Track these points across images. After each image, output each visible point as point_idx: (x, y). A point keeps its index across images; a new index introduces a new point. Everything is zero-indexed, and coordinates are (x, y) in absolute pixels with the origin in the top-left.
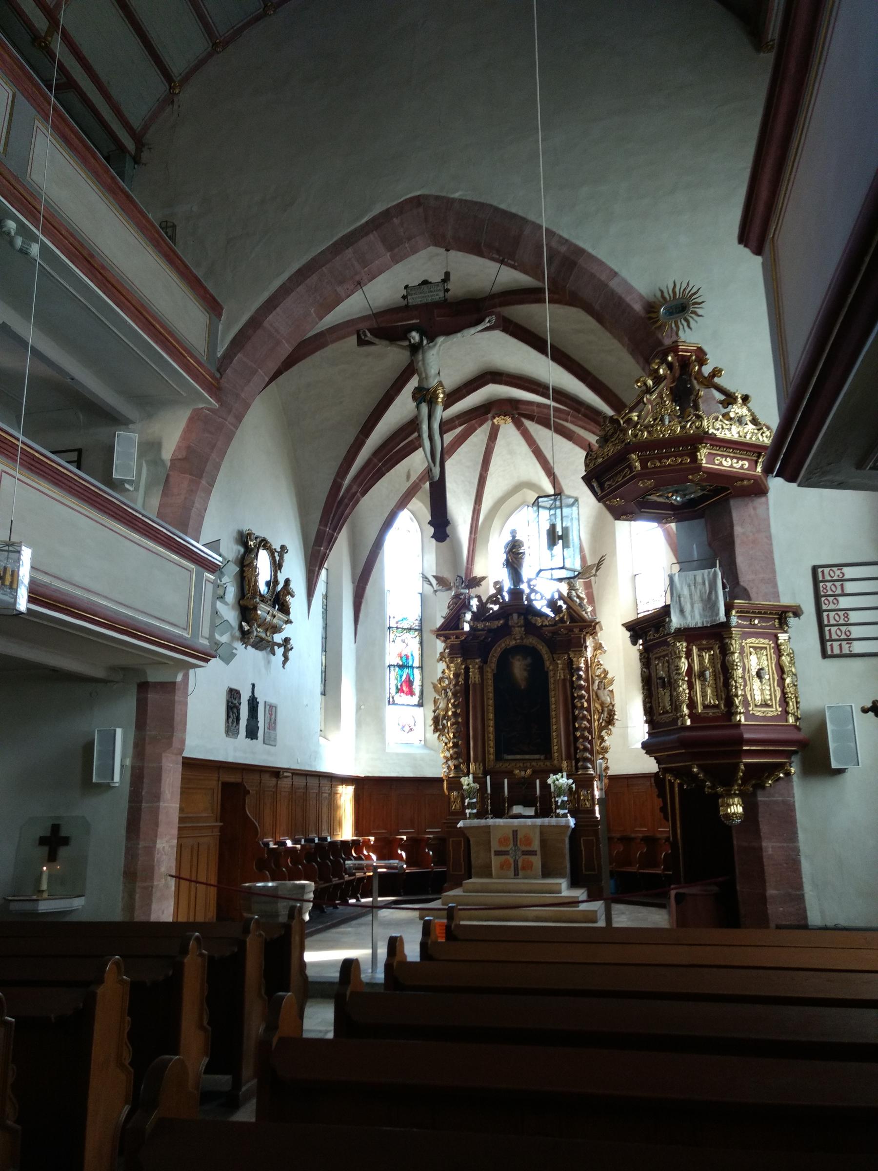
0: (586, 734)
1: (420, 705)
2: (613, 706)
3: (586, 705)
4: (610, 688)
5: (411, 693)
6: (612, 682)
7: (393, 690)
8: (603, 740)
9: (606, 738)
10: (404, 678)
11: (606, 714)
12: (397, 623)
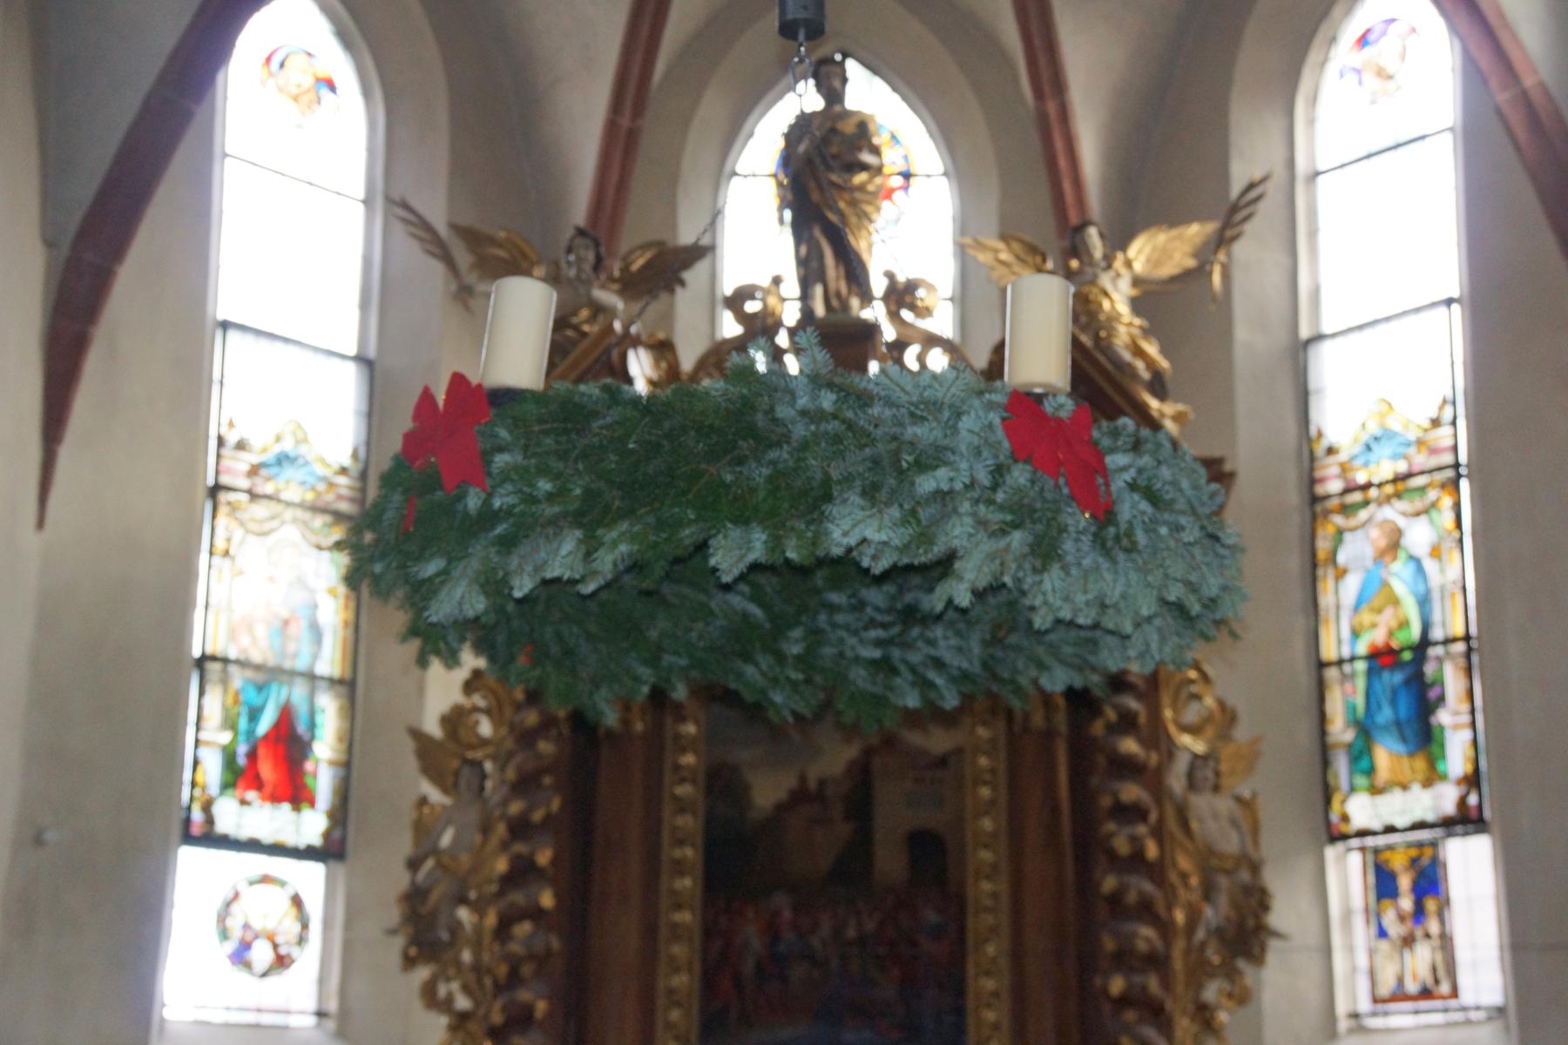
0: (1153, 984)
1: (330, 851)
2: (1255, 868)
3: (1152, 851)
5: (295, 793)
6: (1250, 759)
7: (212, 770)
9: (1223, 1016)
11: (1223, 901)
12: (254, 471)
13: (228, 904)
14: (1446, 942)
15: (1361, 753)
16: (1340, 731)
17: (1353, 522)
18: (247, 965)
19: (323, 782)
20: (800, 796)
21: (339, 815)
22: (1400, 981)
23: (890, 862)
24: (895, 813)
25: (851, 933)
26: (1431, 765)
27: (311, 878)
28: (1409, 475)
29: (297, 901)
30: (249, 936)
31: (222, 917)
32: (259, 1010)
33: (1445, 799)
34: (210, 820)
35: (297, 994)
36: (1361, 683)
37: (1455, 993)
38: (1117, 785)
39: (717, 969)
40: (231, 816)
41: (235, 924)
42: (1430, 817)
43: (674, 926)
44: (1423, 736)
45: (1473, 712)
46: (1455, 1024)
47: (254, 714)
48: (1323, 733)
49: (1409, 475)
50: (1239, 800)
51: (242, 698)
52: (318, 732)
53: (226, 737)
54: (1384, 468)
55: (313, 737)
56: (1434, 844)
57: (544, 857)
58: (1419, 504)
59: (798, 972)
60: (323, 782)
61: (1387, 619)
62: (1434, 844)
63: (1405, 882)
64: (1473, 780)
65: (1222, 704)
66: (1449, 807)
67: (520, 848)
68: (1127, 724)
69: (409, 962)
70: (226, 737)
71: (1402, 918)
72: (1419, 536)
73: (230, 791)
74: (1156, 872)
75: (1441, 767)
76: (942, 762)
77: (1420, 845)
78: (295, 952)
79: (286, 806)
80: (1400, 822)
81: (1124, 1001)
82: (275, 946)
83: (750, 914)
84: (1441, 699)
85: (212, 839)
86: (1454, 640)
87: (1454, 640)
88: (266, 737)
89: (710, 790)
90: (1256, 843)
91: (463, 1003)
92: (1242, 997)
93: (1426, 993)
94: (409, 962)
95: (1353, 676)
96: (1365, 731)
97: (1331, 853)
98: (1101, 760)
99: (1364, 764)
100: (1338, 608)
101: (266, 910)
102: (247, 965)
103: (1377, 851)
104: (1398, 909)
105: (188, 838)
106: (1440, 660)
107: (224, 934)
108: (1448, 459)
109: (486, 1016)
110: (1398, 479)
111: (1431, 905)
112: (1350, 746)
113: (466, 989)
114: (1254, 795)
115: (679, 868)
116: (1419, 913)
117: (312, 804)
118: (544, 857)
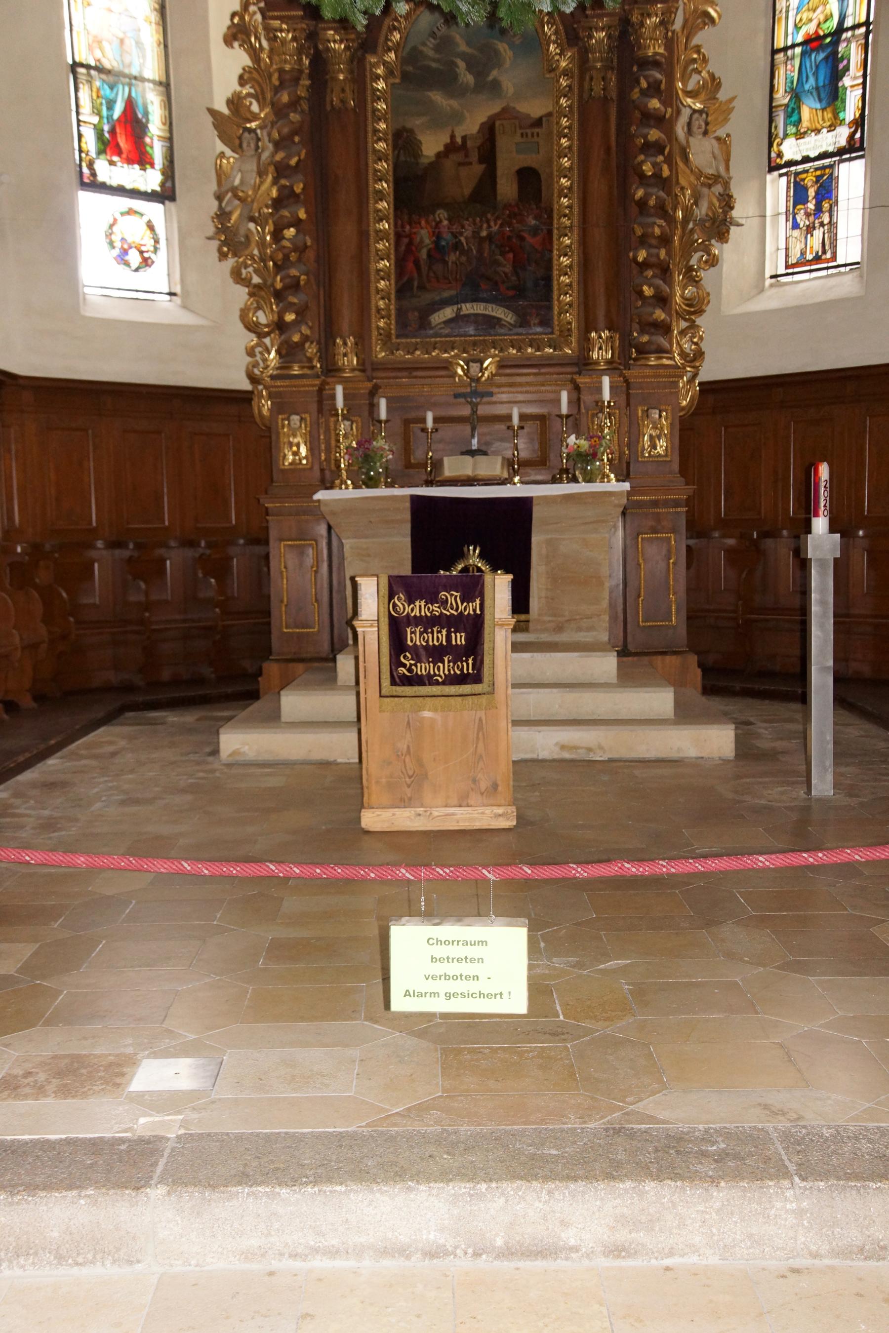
3: (666, 172)
4: (721, 133)
6: (726, 111)
7: (90, 142)
8: (691, 278)
10: (118, 110)
13: (111, 226)
14: (833, 225)
15: (793, 111)
16: (782, 97)
18: (127, 264)
19: (158, 152)
20: (451, 148)
21: (169, 172)
22: (803, 253)
23: (507, 188)
24: (510, 158)
25: (484, 234)
26: (836, 115)
27: (155, 211)
29: (151, 227)
30: (126, 246)
31: (109, 235)
32: (137, 291)
33: (841, 136)
34: (94, 174)
35: (158, 278)
37: (834, 258)
38: (645, 131)
39: (405, 254)
40: (106, 171)
41: (116, 238)
42: (831, 149)
43: (378, 232)
44: (832, 96)
45: (865, 76)
46: (832, 275)
47: (110, 105)
48: (771, 99)
50: (718, 139)
51: (102, 92)
52: (150, 117)
53: (95, 120)
55: (148, 121)
57: (298, 188)
59: (452, 257)
60: (158, 152)
61: (819, 15)
62: (831, 166)
63: (812, 193)
64: (859, 123)
65: (712, 76)
66: (843, 142)
67: (284, 182)
68: (654, 89)
69: (223, 256)
70: (95, 120)
71: (808, 215)
73: (102, 156)
74: (665, 184)
75: (841, 116)
76: (538, 122)
77: (824, 168)
78: (153, 256)
79: (137, 167)
80: (812, 155)
81: (645, 265)
82: (142, 252)
83: (423, 223)
84: (847, 69)
85: (96, 186)
88: (119, 119)
89: (395, 146)
90: (727, 168)
91: (256, 280)
92: (713, 262)
93: (817, 259)
94: (223, 256)
95: (793, 58)
96: (796, 96)
97: (769, 177)
98: (637, 114)
99: (795, 118)
100: (787, 12)
101: (133, 231)
102: (127, 264)
103: (797, 174)
104: (806, 209)
105: (84, 186)
107: (112, 244)
109: (273, 285)
111: (826, 206)
112: (787, 106)
113: (256, 271)
114: (728, 135)
115: (380, 196)
116: (819, 209)
117: (152, 165)
118: (298, 188)
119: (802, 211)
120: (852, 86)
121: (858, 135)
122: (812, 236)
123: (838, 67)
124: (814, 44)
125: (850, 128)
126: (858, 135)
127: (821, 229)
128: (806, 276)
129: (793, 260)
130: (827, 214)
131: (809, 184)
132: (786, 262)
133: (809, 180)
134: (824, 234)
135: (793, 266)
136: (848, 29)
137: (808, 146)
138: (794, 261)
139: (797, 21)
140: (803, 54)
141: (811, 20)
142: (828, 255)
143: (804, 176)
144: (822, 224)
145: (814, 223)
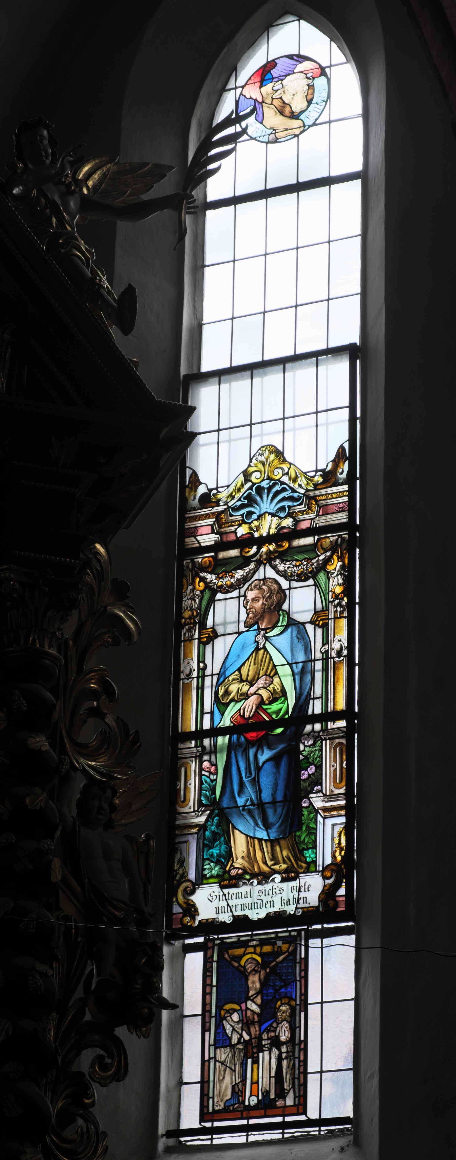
14: (298, 1048)
17: (228, 580)
22: (238, 1091)
26: (298, 852)
28: (296, 533)
36: (221, 760)
42: (291, 909)
45: (349, 795)
49: (296, 533)
54: (268, 526)
56: (293, 940)
58: (304, 567)
62: (293, 940)
63: (254, 982)
64: (340, 871)
66: (313, 898)
71: (246, 1023)
72: (303, 601)
75: (309, 855)
84: (316, 780)
86: (336, 716)
87: (336, 716)
93: (266, 1106)
95: (214, 750)
100: (201, 677)
103: (224, 947)
104: (243, 1013)
106: (316, 737)
108: (342, 518)
110: (279, 536)
112: (203, 827)
116: (268, 1013)
119: (235, 1017)
120: (325, 810)
121: (342, 891)
122: (256, 1061)
123: (299, 775)
124: (252, 735)
125: (325, 878)
126: (342, 891)
127: (275, 1052)
128: (239, 1138)
129: (217, 1104)
130: (285, 1024)
131: (250, 967)
132: (203, 1106)
133: (249, 959)
134: (280, 1060)
135: (217, 1115)
136: (315, 719)
137: (248, 901)
138: (220, 1106)
139: (221, 693)
140: (231, 747)
141: (246, 696)
142: (290, 1101)
143: (239, 951)
144: (276, 1043)
145: (259, 1038)
